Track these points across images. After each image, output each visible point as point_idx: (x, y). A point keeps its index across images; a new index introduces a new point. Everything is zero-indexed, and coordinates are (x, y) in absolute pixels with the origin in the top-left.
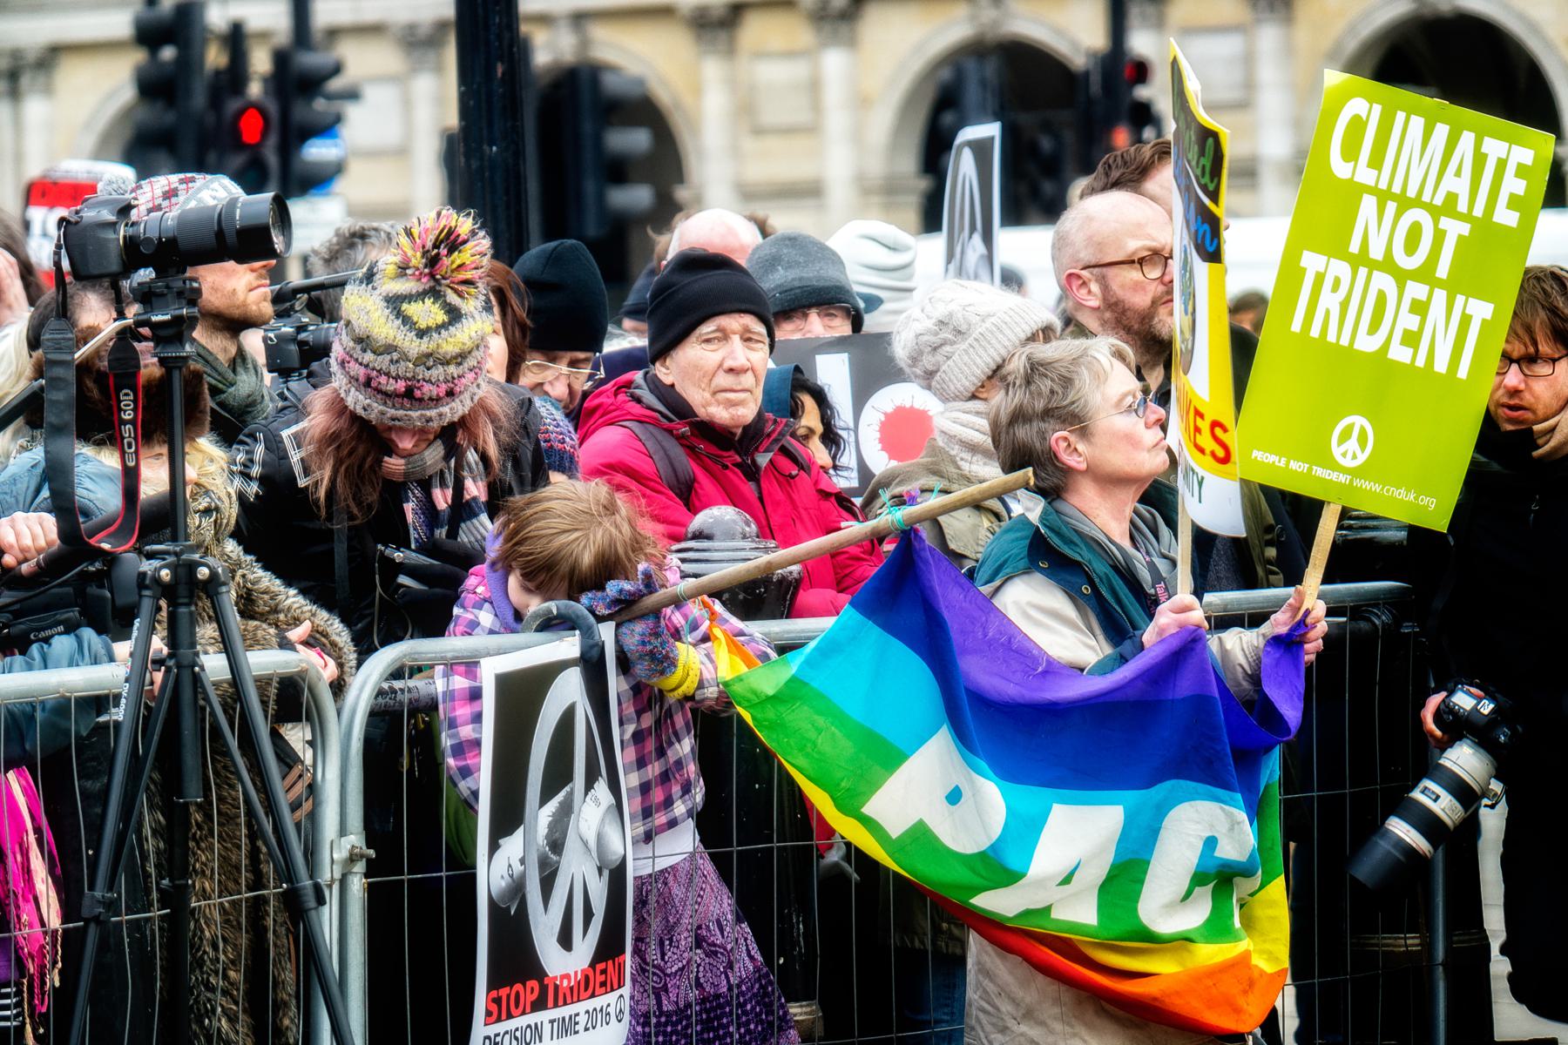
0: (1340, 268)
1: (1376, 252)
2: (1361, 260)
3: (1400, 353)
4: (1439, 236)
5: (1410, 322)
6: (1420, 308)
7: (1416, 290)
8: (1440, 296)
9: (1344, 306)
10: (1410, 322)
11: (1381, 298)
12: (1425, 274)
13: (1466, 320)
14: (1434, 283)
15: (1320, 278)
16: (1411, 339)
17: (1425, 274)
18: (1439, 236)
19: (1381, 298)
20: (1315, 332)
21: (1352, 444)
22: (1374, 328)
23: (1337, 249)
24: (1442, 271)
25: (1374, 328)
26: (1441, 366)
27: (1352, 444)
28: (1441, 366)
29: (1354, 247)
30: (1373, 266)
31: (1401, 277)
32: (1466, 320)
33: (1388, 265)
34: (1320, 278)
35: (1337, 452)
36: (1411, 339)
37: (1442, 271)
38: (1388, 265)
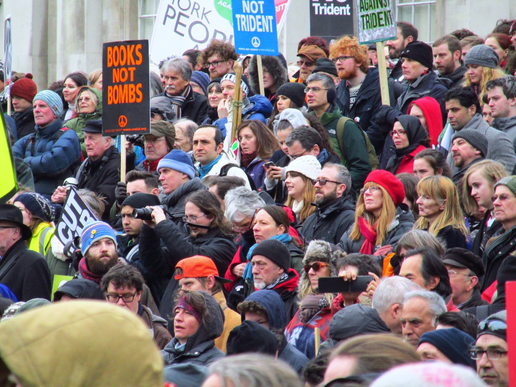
0: (243, 16)
1: (248, 12)
2: (246, 14)
3: (260, 30)
4: (259, 5)
5: (260, 23)
6: (260, 20)
7: (258, 17)
8: (263, 17)
9: (246, 23)
10: (260, 23)
11: (252, 20)
12: (259, 13)
13: (269, 20)
14: (261, 15)
15: (240, 19)
16: (261, 27)
17: (259, 13)
18: (259, 5)
19: (252, 20)
20: (243, 30)
21: (256, 43)
22: (253, 27)
23: (241, 12)
24: (262, 12)
25: (253, 27)
26: (268, 31)
27: (256, 43)
28: (268, 31)
29: (244, 11)
30: (249, 14)
31: (255, 15)
32: (269, 20)
33: (251, 13)
34: (240, 19)
35: (253, 45)
36: (261, 27)
37: (262, 12)
38: (251, 13)
